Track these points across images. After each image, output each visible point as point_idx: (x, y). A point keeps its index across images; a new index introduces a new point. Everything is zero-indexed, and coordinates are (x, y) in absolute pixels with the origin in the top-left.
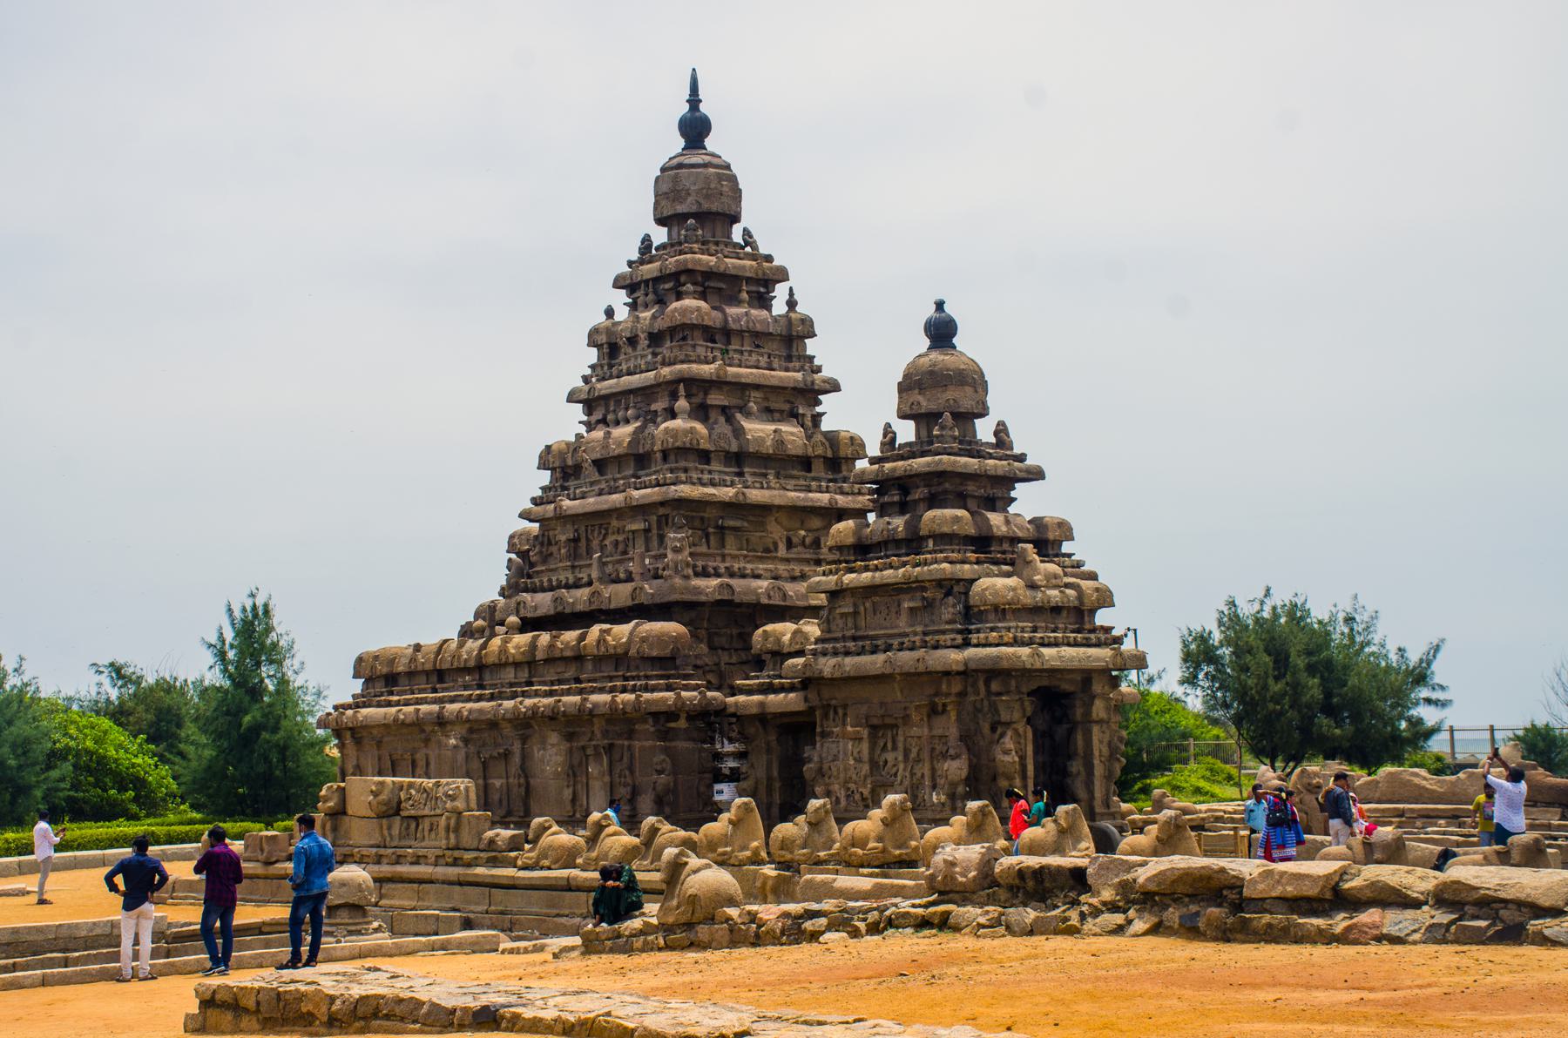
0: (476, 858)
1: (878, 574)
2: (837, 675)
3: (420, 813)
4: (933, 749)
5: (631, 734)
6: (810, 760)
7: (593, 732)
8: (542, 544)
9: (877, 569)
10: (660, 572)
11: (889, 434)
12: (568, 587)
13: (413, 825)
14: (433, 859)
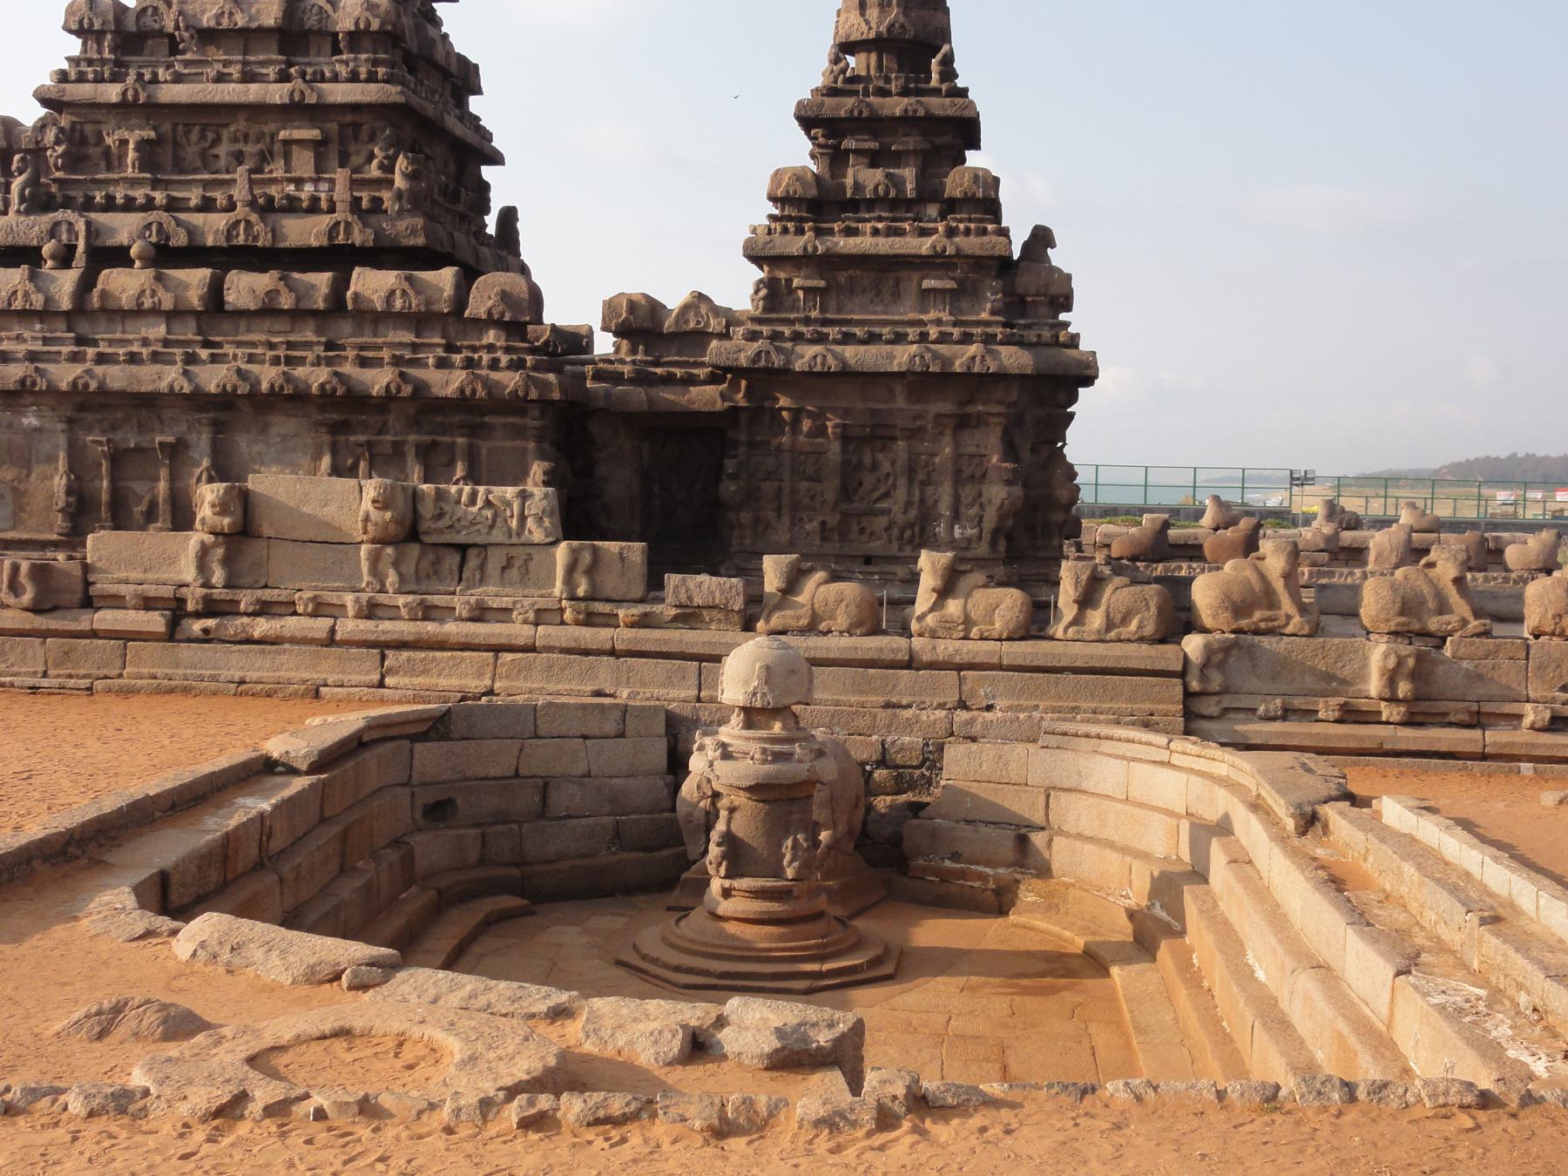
0: (646, 615)
1: (881, 240)
2: (818, 368)
3: (479, 540)
4: (958, 471)
5: (475, 431)
6: (734, 477)
7: (385, 423)
8: (70, 141)
9: (876, 232)
10: (365, 204)
11: (836, 60)
12: (149, 205)
13: (457, 558)
14: (531, 616)
